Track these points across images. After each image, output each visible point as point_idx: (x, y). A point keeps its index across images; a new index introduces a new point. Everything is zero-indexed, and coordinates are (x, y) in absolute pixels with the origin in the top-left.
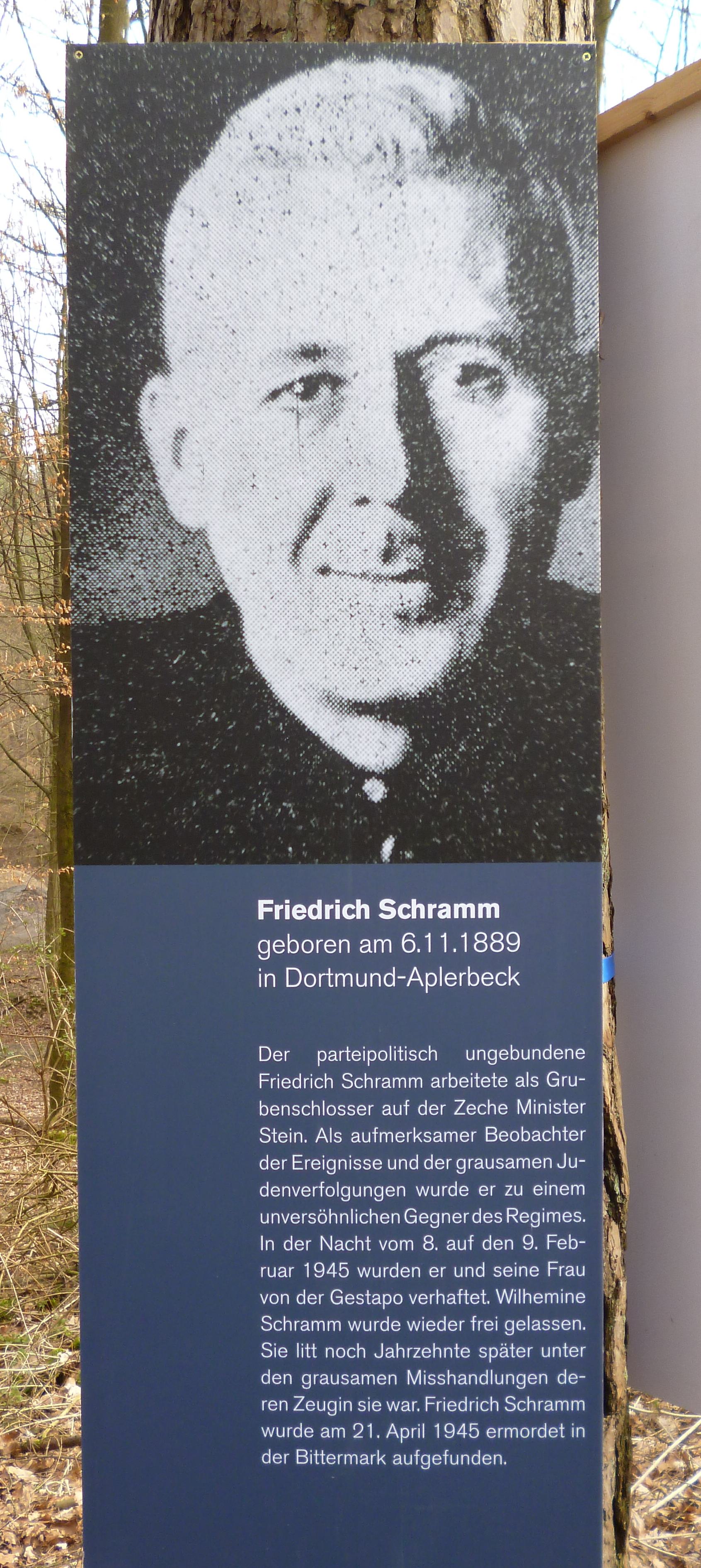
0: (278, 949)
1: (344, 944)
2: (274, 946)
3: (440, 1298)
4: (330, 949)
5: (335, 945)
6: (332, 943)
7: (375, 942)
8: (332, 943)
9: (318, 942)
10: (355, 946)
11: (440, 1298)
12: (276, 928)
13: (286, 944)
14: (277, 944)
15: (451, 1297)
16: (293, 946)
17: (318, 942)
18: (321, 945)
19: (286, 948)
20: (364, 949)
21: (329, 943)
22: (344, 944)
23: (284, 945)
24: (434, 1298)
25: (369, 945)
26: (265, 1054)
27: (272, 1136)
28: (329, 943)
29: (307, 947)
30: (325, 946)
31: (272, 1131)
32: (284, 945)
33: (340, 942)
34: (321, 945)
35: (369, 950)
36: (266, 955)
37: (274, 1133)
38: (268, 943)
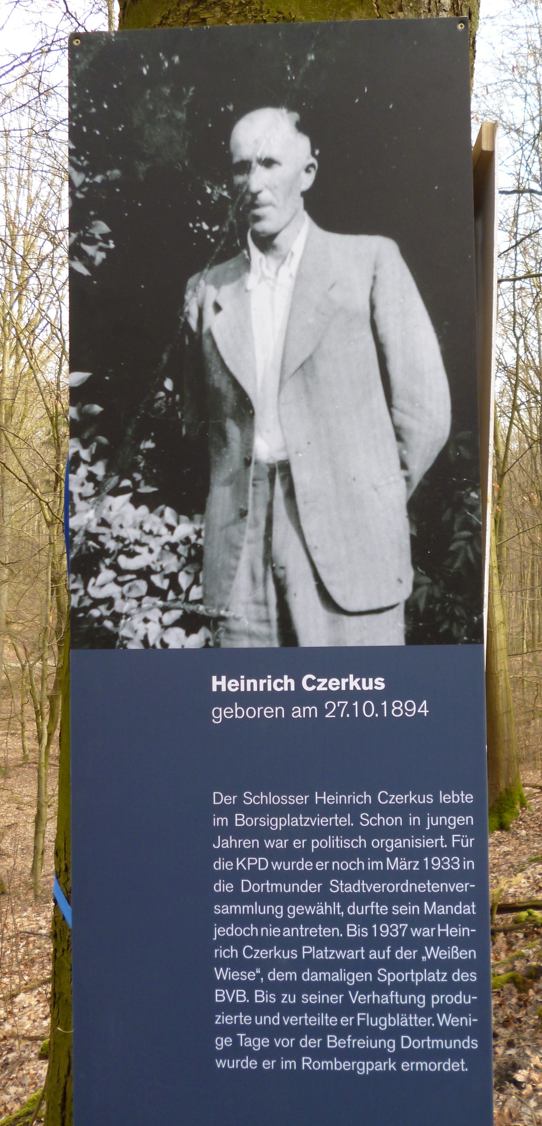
2: (225, 712)
3: (376, 998)
4: (268, 714)
5: (272, 712)
6: (270, 710)
7: (304, 709)
8: (270, 710)
10: (288, 712)
11: (376, 998)
12: (226, 699)
14: (227, 710)
15: (385, 997)
17: (259, 709)
18: (262, 711)
19: (234, 714)
20: (295, 715)
23: (232, 712)
24: (371, 998)
25: (299, 711)
26: (218, 798)
27: (340, 886)
29: (251, 712)
30: (265, 712)
31: (340, 883)
32: (232, 712)
34: (262, 711)
36: (218, 720)
37: (341, 884)
38: (220, 709)
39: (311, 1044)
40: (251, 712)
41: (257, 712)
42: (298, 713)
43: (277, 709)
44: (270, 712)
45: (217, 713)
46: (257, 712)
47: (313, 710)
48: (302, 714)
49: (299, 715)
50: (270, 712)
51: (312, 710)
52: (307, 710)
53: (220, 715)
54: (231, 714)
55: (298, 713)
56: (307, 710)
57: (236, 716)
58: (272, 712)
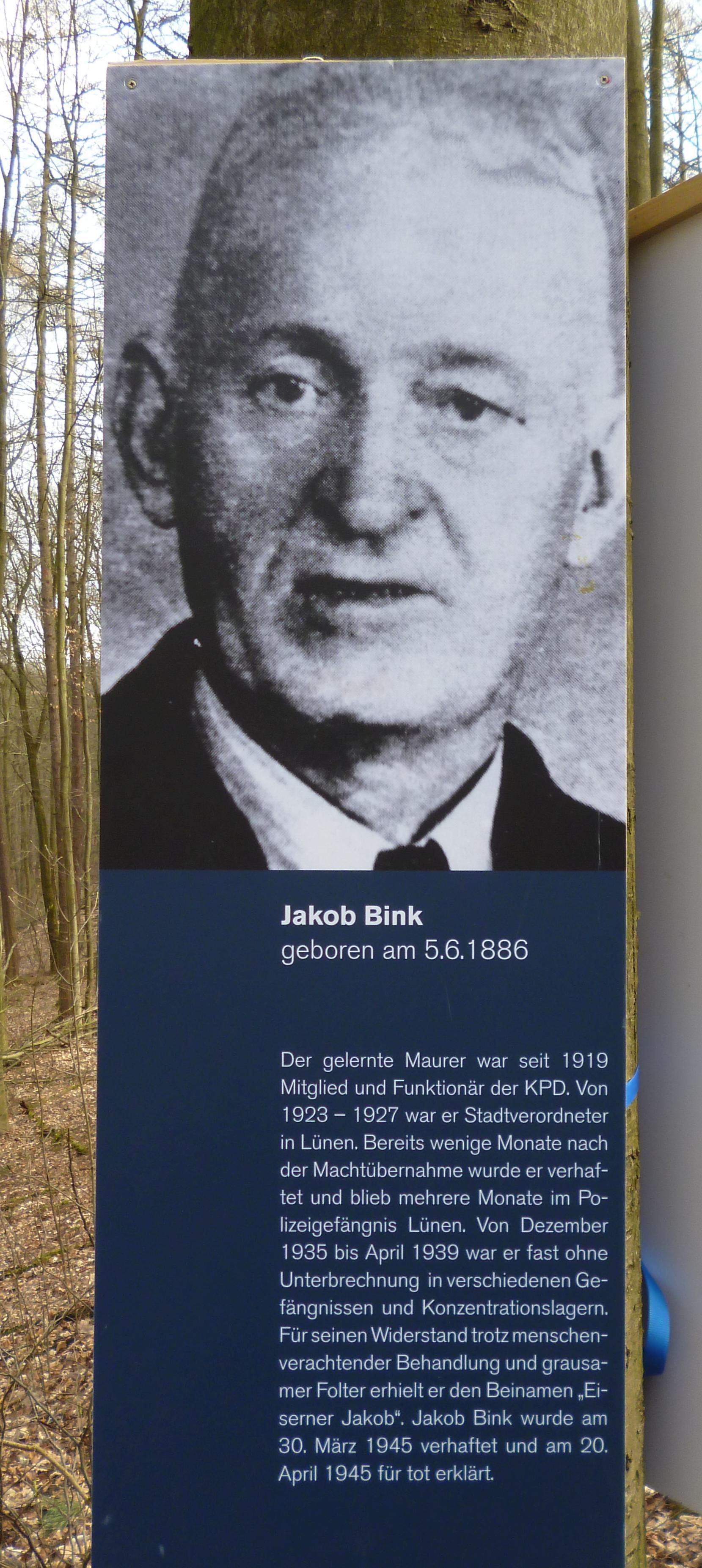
0: (302, 954)
1: (368, 950)
2: (298, 951)
4: (353, 954)
5: (359, 951)
6: (355, 949)
7: (399, 948)
8: (355, 949)
9: (342, 948)
10: (379, 952)
13: (310, 949)
16: (317, 952)
17: (342, 948)
18: (345, 950)
20: (388, 955)
21: (353, 949)
22: (368, 950)
25: (393, 951)
26: (288, 1059)
28: (353, 949)
29: (331, 952)
30: (349, 951)
33: (364, 948)
34: (345, 950)
35: (393, 956)
36: (289, 961)
38: (292, 948)
39: (408, 1339)
40: (331, 952)
41: (339, 951)
42: (391, 953)
43: (364, 948)
44: (355, 951)
45: (288, 951)
46: (339, 951)
47: (410, 950)
48: (396, 955)
49: (393, 956)
50: (355, 951)
51: (408, 950)
52: (402, 950)
53: (292, 954)
54: (306, 953)
55: (391, 953)
56: (402, 950)
57: (313, 956)
58: (359, 951)
